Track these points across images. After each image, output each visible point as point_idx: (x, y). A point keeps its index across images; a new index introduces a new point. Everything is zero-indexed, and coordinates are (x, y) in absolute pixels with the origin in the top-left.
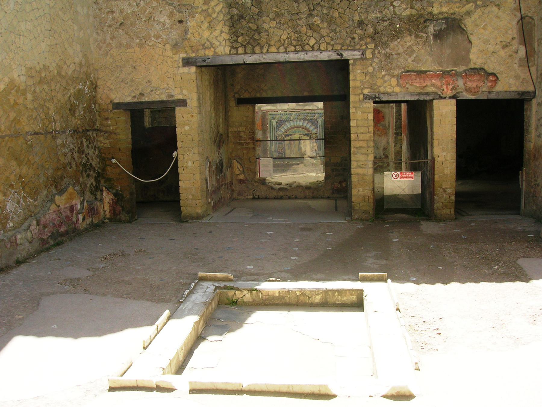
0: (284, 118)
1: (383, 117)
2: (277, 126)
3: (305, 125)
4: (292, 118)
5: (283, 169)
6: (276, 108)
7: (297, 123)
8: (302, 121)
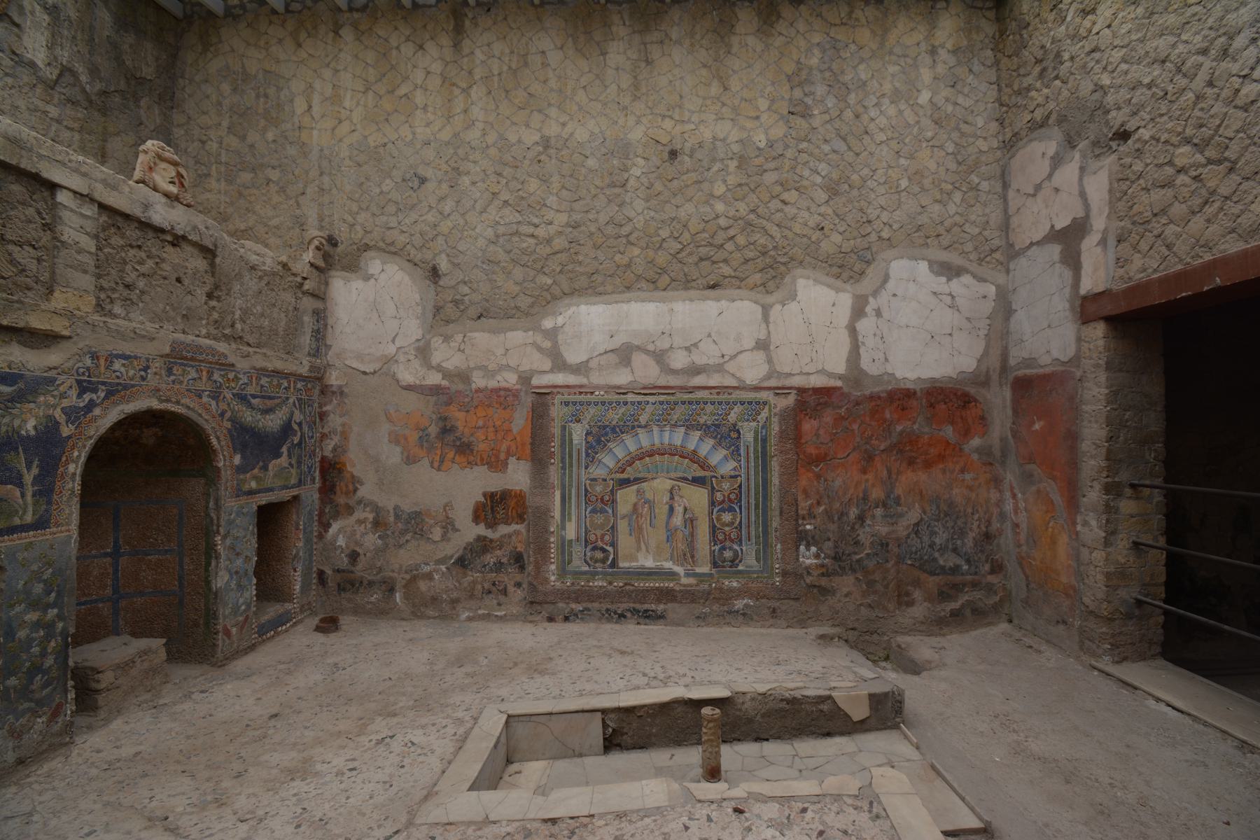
0: (614, 416)
1: (983, 418)
2: (589, 446)
3: (691, 446)
4: (643, 419)
5: (607, 610)
6: (584, 381)
7: (661, 436)
8: (683, 429)
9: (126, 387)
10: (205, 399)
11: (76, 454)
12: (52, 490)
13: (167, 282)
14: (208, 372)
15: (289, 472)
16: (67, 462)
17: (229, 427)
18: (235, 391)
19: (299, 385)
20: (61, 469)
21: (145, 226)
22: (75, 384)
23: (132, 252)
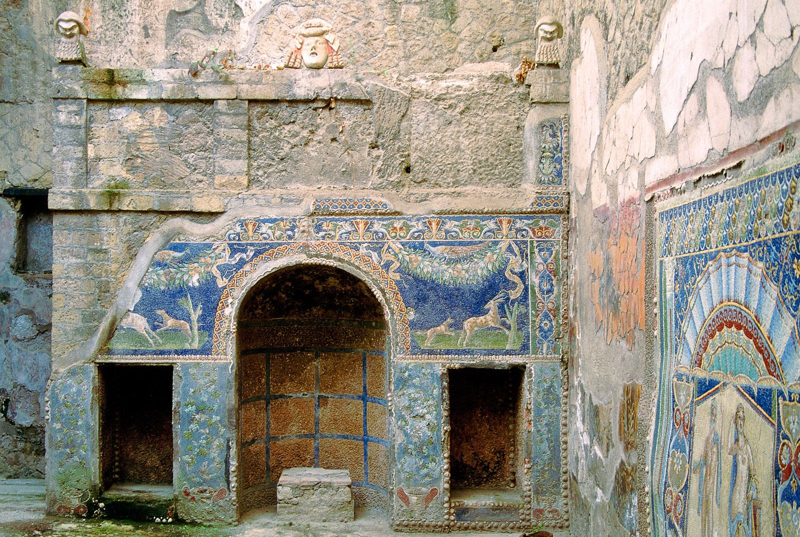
9: (272, 246)
10: (363, 251)
11: (230, 300)
12: (212, 327)
13: (322, 145)
14: (366, 224)
15: (504, 334)
16: (223, 308)
17: (398, 278)
18: (403, 240)
19: (519, 225)
20: (219, 312)
21: (294, 102)
22: (227, 247)
23: (287, 128)
